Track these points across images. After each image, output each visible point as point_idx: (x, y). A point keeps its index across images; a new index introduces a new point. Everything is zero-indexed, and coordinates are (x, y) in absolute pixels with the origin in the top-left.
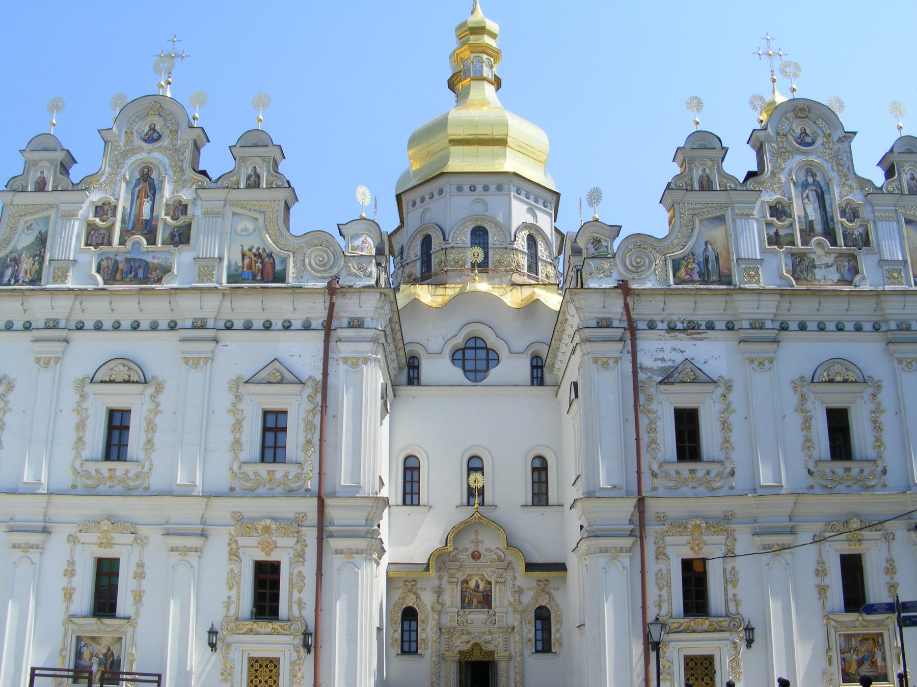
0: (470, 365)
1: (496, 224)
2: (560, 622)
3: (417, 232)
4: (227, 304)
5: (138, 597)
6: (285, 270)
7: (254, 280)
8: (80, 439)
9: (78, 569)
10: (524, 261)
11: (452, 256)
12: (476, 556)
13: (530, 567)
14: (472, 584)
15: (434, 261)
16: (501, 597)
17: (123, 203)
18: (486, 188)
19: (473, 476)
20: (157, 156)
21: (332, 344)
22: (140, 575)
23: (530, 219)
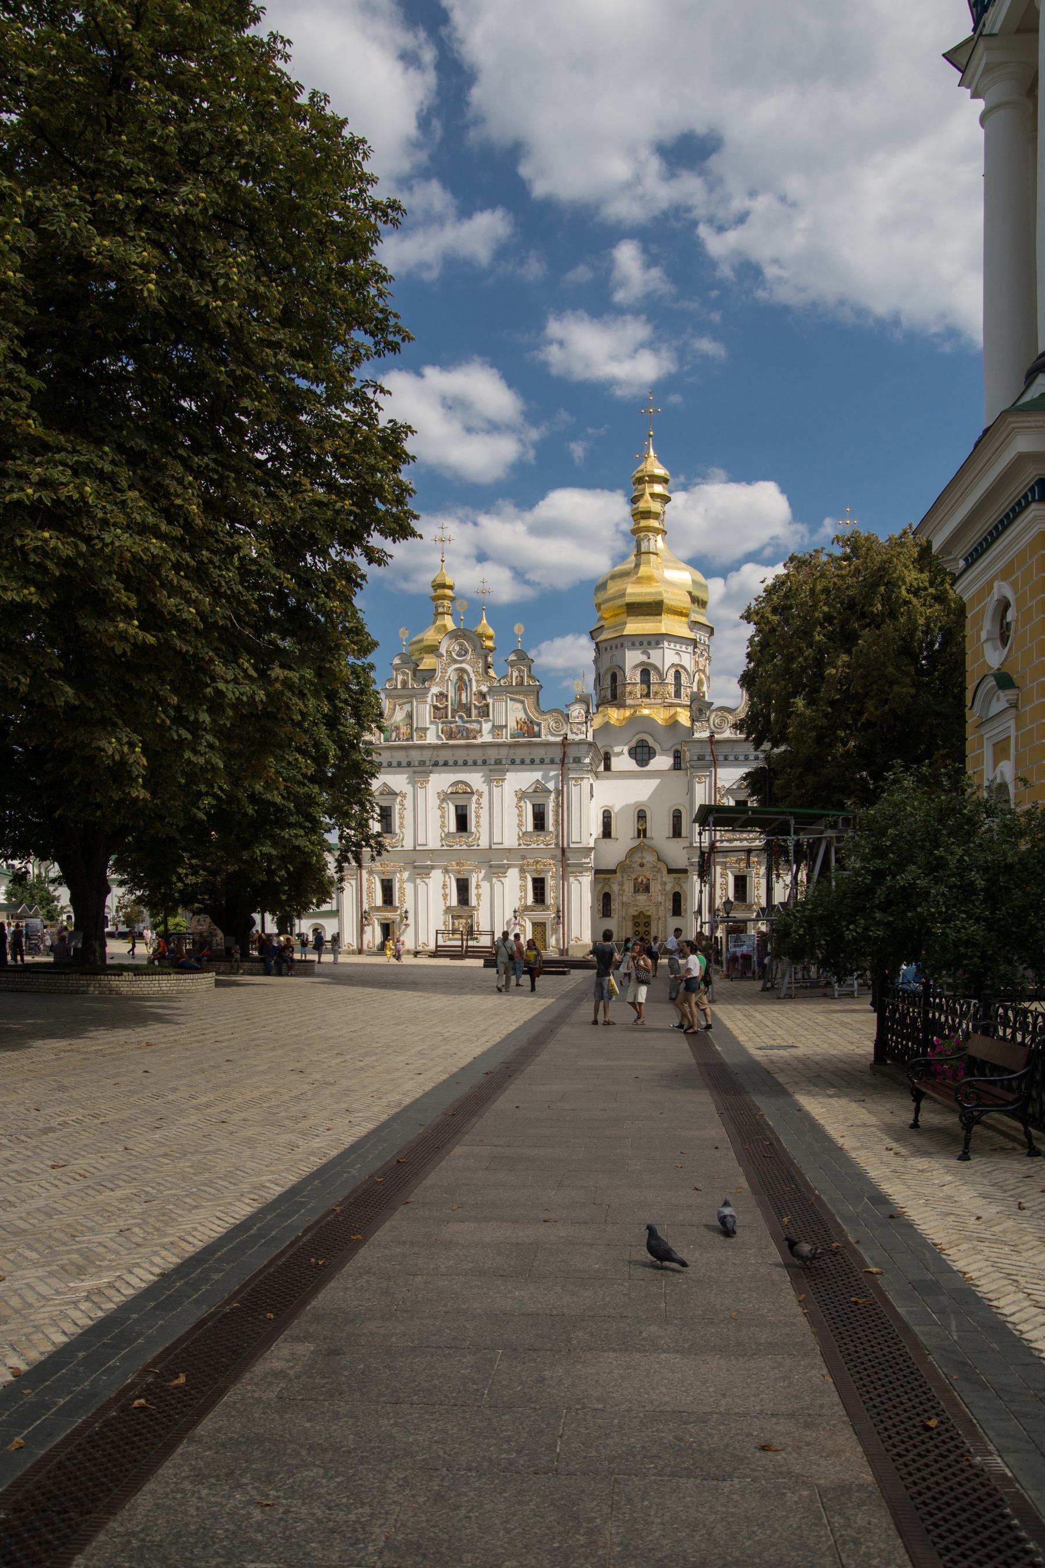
0: (639, 757)
1: (656, 668)
2: (686, 900)
3: (608, 669)
4: (512, 751)
5: (478, 896)
6: (540, 730)
7: (524, 737)
8: (443, 822)
9: (448, 884)
10: (672, 689)
11: (628, 689)
12: (642, 865)
13: (670, 871)
14: (640, 880)
15: (619, 691)
16: (655, 887)
17: (451, 694)
18: (649, 643)
19: (641, 822)
20: (464, 665)
21: (565, 771)
22: (478, 886)
23: (676, 660)
